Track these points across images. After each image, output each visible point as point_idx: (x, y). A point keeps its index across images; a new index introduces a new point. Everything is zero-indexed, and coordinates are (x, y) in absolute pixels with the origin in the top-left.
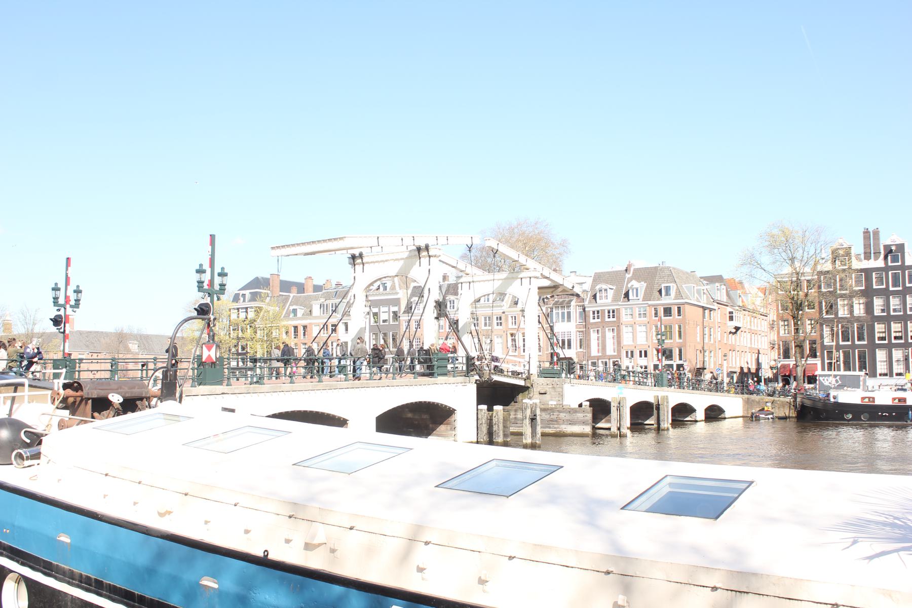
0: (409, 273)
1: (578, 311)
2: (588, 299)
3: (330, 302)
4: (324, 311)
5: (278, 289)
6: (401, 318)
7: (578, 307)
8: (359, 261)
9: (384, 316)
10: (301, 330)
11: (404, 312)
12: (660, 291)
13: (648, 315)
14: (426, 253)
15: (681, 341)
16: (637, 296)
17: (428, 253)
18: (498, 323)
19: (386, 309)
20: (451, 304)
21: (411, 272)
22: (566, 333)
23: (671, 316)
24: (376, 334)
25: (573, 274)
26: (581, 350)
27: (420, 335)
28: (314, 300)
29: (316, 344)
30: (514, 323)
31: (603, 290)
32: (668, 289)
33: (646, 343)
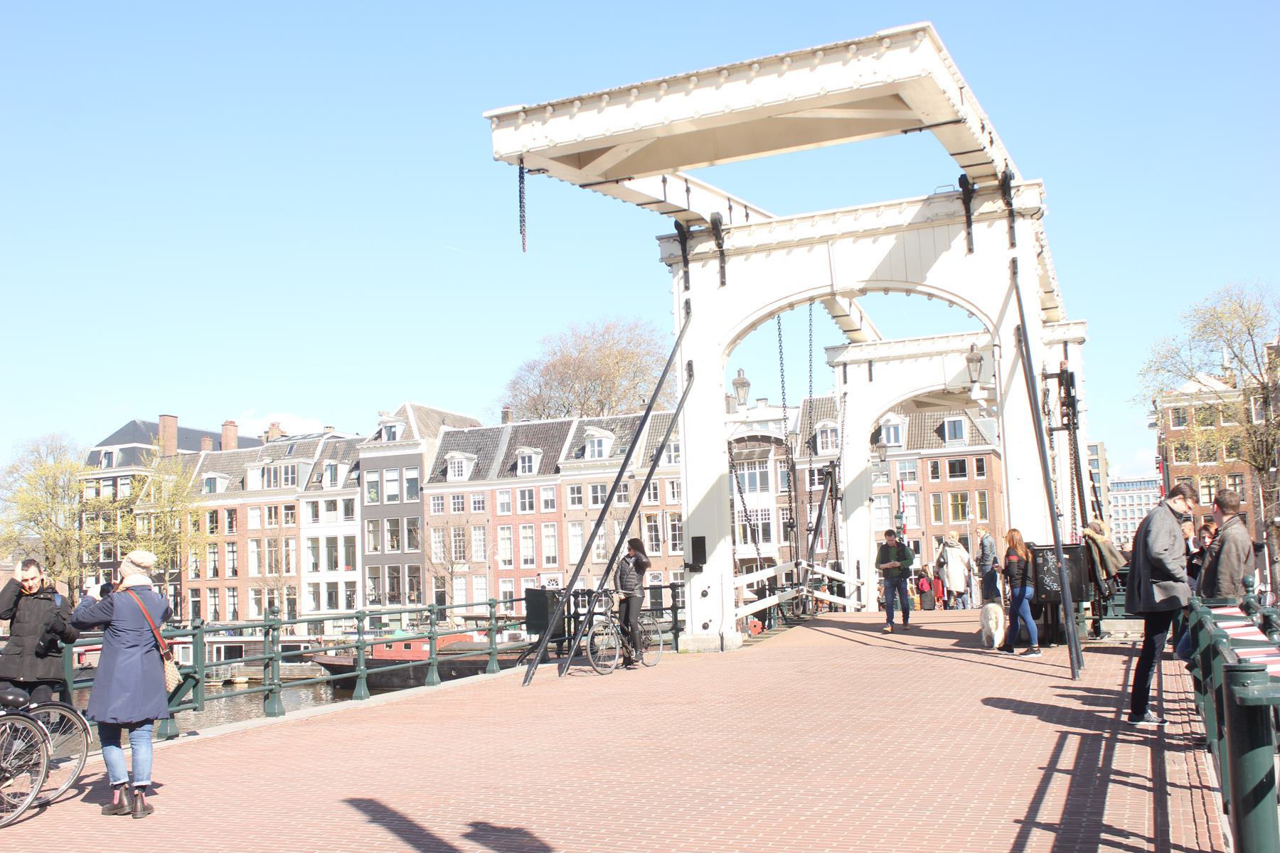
0: (926, 278)
1: (779, 470)
2: (798, 449)
3: (282, 464)
4: (269, 481)
5: (175, 442)
6: (424, 492)
7: (778, 463)
8: (709, 246)
9: (390, 489)
10: (224, 518)
11: (431, 480)
12: (940, 431)
13: (919, 475)
14: (999, 204)
15: (939, 524)
16: (897, 440)
17: (1009, 204)
18: (573, 500)
19: (395, 475)
20: (524, 462)
21: (928, 275)
22: (759, 513)
23: (965, 476)
24: (375, 523)
25: (761, 404)
26: (787, 544)
27: (465, 521)
28: (248, 461)
29: (255, 543)
30: (652, 495)
31: (829, 431)
32: (956, 426)
33: (918, 527)
